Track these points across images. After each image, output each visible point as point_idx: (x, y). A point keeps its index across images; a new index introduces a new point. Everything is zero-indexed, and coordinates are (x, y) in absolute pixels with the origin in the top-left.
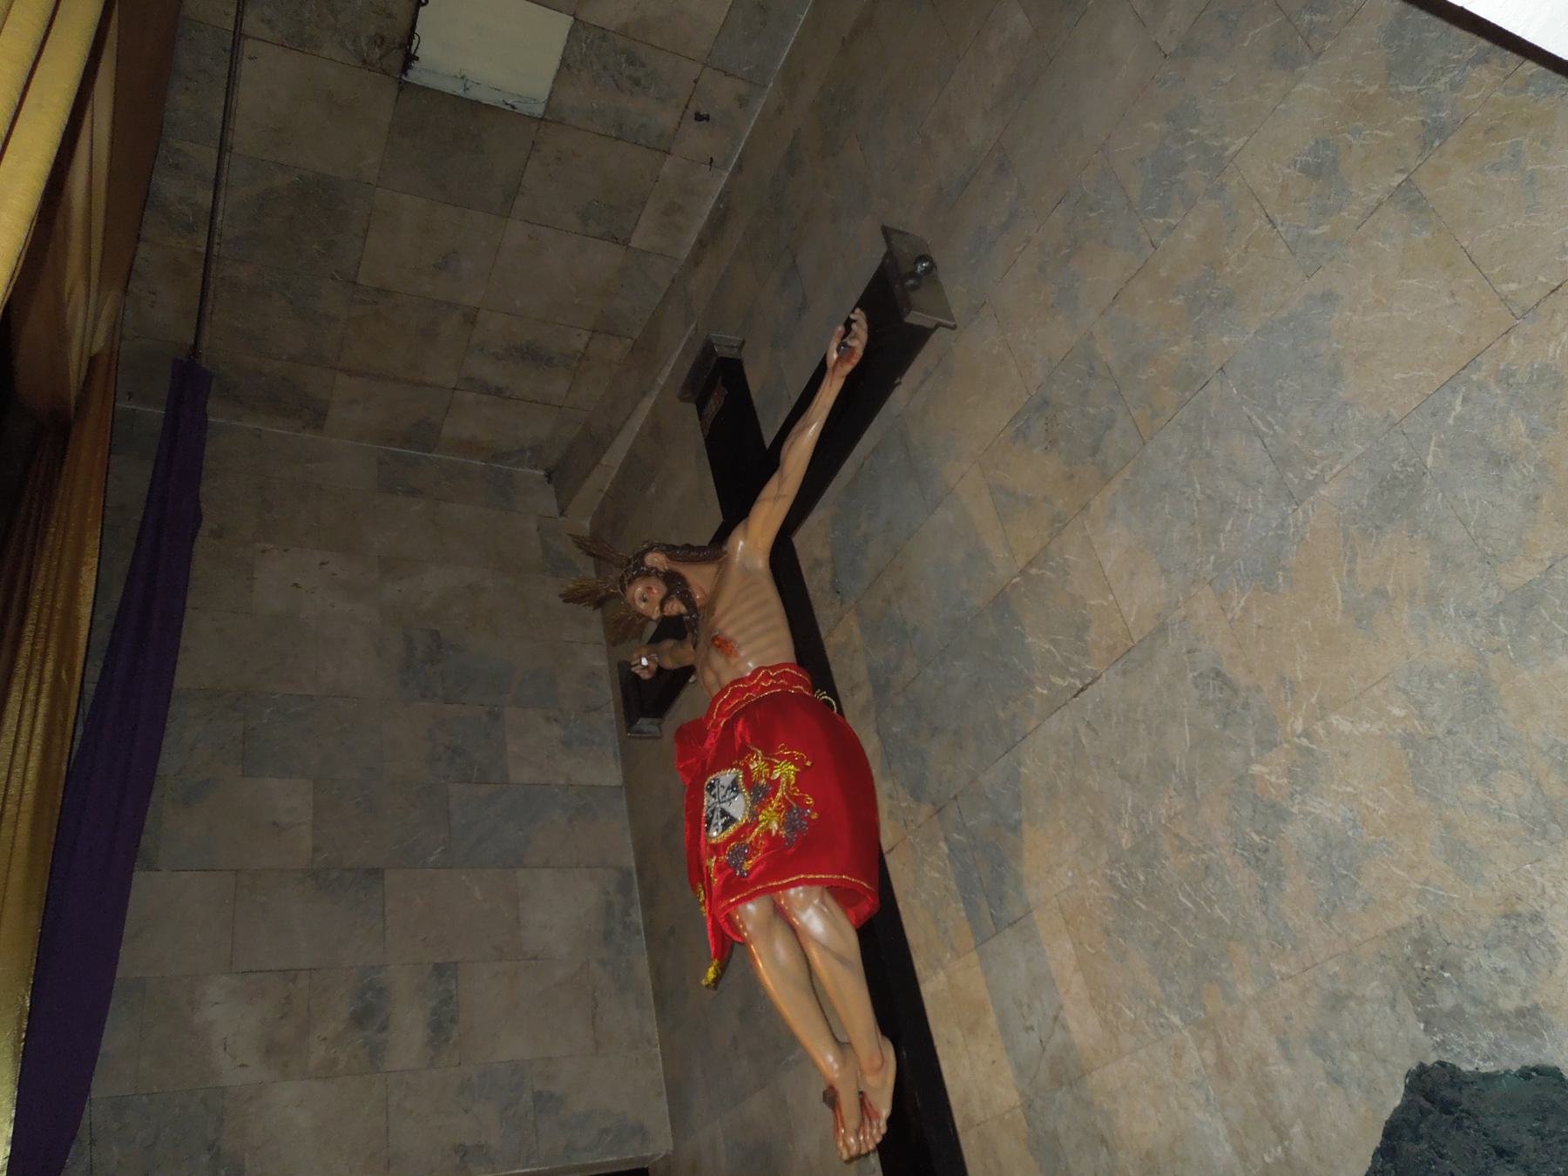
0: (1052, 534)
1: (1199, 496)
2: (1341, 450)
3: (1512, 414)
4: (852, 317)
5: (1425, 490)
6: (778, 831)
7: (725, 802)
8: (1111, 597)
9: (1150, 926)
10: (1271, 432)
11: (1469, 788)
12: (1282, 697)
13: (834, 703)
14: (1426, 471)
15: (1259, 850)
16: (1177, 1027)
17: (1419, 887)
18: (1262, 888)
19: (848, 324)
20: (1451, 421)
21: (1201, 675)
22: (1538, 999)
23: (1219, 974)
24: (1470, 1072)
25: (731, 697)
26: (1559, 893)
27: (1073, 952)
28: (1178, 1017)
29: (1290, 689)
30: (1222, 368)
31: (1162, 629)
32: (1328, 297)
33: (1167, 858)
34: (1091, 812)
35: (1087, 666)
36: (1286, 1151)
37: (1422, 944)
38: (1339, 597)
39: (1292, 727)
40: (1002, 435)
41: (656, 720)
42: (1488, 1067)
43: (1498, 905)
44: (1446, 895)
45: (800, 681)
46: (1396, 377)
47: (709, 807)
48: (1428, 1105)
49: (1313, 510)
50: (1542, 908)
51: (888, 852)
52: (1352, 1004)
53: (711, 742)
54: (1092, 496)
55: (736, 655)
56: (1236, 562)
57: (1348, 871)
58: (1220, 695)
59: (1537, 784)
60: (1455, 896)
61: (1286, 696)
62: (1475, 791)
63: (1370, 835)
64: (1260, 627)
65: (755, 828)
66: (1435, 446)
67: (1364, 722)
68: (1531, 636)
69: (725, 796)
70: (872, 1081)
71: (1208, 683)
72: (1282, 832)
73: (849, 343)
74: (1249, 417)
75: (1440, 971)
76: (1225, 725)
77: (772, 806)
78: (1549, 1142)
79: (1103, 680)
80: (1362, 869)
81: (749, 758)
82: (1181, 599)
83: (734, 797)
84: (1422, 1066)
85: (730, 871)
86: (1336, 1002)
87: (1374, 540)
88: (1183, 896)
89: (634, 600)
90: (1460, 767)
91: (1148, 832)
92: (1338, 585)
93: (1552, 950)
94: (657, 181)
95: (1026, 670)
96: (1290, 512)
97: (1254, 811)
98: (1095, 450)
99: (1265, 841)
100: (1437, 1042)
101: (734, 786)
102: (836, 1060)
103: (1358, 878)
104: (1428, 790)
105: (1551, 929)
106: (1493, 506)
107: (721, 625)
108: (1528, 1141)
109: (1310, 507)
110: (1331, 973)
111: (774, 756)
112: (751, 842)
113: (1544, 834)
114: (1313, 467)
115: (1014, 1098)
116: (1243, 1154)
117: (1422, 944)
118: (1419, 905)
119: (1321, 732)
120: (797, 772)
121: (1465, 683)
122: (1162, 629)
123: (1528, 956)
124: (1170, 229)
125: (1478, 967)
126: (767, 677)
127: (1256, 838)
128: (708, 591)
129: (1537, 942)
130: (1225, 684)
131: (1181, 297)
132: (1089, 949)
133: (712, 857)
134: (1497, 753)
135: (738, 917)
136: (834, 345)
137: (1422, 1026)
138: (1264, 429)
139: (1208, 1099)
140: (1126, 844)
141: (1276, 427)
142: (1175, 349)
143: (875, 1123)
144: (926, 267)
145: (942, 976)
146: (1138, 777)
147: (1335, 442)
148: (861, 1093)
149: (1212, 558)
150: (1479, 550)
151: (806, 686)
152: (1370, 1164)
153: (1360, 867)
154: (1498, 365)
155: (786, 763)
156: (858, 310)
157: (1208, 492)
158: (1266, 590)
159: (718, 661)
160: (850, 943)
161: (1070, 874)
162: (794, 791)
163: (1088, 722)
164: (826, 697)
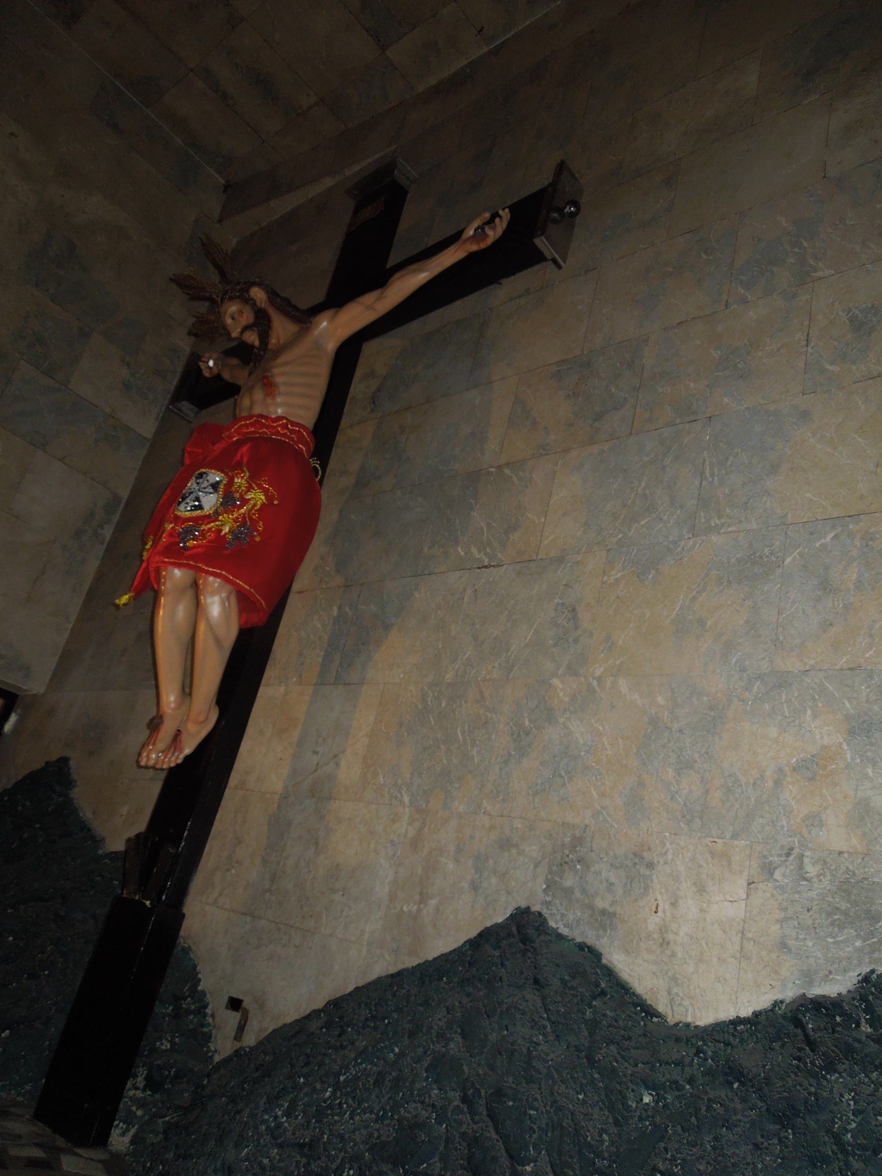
0: (534, 454)
1: (640, 490)
2: (743, 519)
3: (855, 564)
4: (501, 212)
5: (773, 577)
6: (226, 534)
7: (202, 492)
8: (543, 520)
9: (429, 737)
10: (711, 479)
11: (668, 770)
12: (601, 648)
13: (320, 473)
14: (781, 565)
15: (523, 731)
16: (404, 804)
17: (599, 808)
18: (510, 755)
19: (495, 215)
20: (818, 545)
21: (563, 604)
22: (619, 910)
23: (450, 788)
24: (552, 927)
25: (252, 425)
26: (673, 859)
27: (372, 724)
28: (409, 798)
29: (608, 646)
30: (710, 417)
31: (559, 560)
32: (805, 415)
33: (466, 702)
34: (440, 646)
35: (499, 554)
36: (419, 910)
37: (578, 841)
38: (677, 610)
39: (594, 670)
40: (547, 367)
41: (196, 409)
42: (564, 931)
43: (635, 846)
44: (610, 821)
45: (305, 443)
46: (807, 495)
47: (190, 489)
48: (515, 932)
49: (700, 546)
50: (658, 862)
51: (298, 592)
52: (514, 851)
53: (218, 447)
54: (575, 446)
55: (274, 398)
56: (632, 547)
57: (566, 775)
58: (566, 624)
59: (707, 791)
60: (616, 826)
61: (604, 650)
62: (670, 773)
63: (593, 762)
64: (618, 597)
65: (213, 522)
66: (798, 553)
67: (637, 694)
68: (766, 704)
69: (205, 488)
70: (191, 727)
71: (564, 612)
72: (544, 729)
73: (486, 229)
74: (704, 461)
75: (576, 863)
76: (556, 645)
77: (233, 515)
78: (567, 991)
79: (503, 569)
80: (574, 779)
81: (238, 473)
82: (584, 549)
83: (211, 493)
84: (528, 908)
85: (178, 540)
86: (505, 844)
87: (722, 587)
88: (460, 731)
89: (225, 313)
90: (671, 754)
91: (466, 680)
92: (681, 601)
93: (647, 888)
94: (434, 16)
95: (459, 532)
96: (686, 538)
97: (537, 707)
98: (598, 417)
99: (531, 728)
100: (546, 900)
101: (215, 486)
102: (175, 701)
103: (569, 783)
104: (644, 756)
105: (654, 877)
106: (803, 613)
107: (275, 371)
108: (556, 983)
109: (700, 542)
110: (514, 826)
111: (254, 482)
112: (204, 530)
113: (689, 823)
114: (720, 517)
115: (279, 787)
116: (392, 897)
117: (578, 841)
118: (591, 819)
119: (609, 684)
120: (264, 503)
121: (710, 707)
122: (559, 560)
123: (631, 883)
124: (744, 301)
125: (598, 873)
126: (285, 426)
127: (527, 722)
128: (282, 342)
129: (641, 880)
130: (574, 619)
131: (719, 352)
132: (383, 728)
133: (171, 524)
134: (698, 759)
135: (164, 573)
136: (476, 224)
137: (544, 886)
138: (708, 474)
139: (394, 855)
140: (448, 679)
141: (716, 478)
142: (692, 385)
143: (176, 754)
144: (572, 212)
145: (282, 689)
146: (482, 643)
147: (743, 511)
148: (179, 731)
149: (620, 536)
150: (776, 633)
151: (308, 450)
152: (460, 944)
153: (574, 776)
154: (870, 528)
155: (260, 492)
156: (507, 210)
157: (647, 492)
158: (638, 577)
159: (258, 394)
160: (230, 635)
161: (402, 676)
162: (255, 514)
163: (476, 589)
164: (318, 466)
